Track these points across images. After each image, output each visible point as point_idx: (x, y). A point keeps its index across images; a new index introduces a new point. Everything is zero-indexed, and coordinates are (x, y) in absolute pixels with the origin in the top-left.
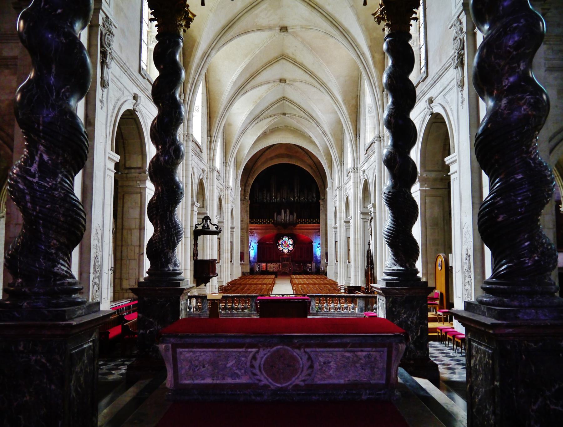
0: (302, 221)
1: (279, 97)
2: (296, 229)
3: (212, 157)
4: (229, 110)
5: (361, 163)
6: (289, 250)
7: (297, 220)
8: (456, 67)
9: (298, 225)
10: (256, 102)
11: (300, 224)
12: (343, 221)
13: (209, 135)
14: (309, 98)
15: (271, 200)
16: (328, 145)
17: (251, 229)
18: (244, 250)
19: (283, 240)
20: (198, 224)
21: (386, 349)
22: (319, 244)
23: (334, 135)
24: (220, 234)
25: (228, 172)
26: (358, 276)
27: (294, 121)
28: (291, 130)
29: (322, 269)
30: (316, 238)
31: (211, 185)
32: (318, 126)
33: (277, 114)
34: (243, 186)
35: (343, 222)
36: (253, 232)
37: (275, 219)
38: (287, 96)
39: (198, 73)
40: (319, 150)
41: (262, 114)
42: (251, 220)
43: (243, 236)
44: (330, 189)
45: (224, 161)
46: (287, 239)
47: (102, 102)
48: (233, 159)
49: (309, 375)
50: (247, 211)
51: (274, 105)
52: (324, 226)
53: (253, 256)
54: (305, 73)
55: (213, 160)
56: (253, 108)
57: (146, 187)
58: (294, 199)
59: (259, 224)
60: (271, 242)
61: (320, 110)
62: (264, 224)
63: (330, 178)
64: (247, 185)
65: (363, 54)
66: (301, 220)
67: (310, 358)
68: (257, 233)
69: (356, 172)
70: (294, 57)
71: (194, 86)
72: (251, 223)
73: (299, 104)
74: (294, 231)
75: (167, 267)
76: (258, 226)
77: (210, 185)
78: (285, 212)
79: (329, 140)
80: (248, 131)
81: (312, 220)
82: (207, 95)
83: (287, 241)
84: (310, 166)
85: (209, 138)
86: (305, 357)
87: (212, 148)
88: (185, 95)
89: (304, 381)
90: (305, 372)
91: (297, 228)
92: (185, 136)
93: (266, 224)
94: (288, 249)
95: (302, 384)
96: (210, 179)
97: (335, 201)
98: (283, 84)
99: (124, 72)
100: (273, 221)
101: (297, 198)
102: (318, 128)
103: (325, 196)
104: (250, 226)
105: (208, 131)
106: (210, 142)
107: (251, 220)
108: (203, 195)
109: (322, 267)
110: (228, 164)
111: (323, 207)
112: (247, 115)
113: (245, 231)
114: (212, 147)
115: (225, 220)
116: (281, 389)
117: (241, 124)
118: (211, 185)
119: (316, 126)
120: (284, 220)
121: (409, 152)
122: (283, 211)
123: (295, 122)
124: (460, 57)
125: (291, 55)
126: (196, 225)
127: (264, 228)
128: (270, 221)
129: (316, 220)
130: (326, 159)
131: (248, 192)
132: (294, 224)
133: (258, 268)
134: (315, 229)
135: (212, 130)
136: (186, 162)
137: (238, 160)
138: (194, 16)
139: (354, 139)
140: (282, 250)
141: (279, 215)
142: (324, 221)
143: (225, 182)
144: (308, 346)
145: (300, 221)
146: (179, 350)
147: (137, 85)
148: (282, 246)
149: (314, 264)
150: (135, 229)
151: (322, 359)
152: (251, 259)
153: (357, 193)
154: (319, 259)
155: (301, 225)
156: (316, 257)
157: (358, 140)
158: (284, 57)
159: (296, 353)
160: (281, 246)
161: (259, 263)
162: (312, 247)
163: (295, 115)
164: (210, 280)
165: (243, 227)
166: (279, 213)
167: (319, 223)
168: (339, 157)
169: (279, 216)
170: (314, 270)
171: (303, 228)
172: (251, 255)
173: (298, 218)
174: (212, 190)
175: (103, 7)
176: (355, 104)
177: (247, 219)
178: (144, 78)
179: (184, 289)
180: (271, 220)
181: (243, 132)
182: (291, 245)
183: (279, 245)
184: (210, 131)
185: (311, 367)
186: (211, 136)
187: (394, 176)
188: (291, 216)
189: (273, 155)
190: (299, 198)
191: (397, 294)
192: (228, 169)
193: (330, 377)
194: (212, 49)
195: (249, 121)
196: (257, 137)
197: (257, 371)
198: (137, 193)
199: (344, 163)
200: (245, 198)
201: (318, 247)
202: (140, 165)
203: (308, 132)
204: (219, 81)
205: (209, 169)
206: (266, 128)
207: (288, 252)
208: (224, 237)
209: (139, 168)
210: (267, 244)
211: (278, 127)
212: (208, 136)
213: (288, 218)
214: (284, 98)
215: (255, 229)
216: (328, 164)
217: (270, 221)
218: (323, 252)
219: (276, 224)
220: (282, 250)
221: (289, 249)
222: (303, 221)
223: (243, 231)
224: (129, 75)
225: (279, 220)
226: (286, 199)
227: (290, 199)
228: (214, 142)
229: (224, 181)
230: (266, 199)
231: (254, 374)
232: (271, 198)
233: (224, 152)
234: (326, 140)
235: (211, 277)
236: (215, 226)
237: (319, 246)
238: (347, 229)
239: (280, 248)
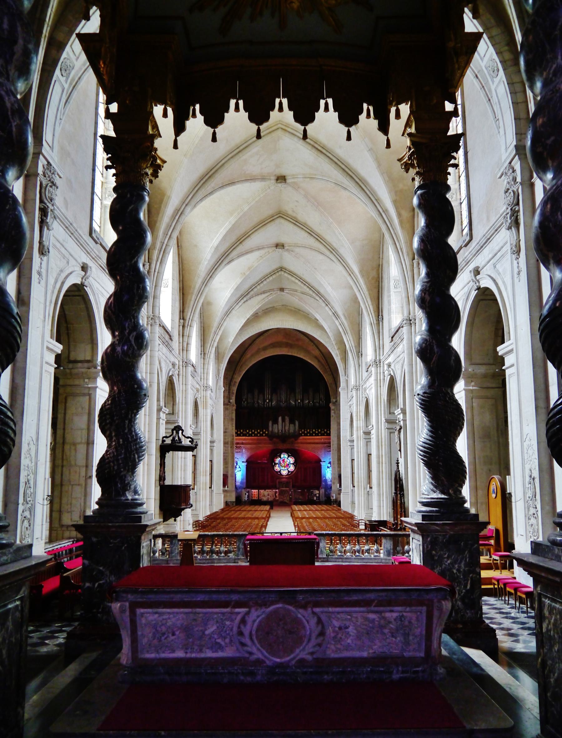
0: (306, 432)
1: (274, 267)
2: (298, 443)
3: (185, 346)
4: (209, 284)
5: (385, 354)
6: (289, 471)
7: (299, 431)
8: (509, 228)
9: (301, 438)
10: (244, 274)
11: (304, 436)
12: (362, 431)
13: (182, 318)
14: (315, 269)
15: (264, 404)
16: (341, 330)
17: (237, 443)
18: (227, 472)
19: (281, 458)
20: (166, 437)
21: (424, 608)
22: (330, 463)
23: (348, 317)
24: (195, 450)
25: (206, 366)
26: (383, 506)
27: (295, 299)
28: (291, 310)
29: (334, 498)
30: (325, 454)
31: (184, 383)
32: (327, 305)
33: (272, 290)
34: (227, 385)
35: (362, 433)
36: (240, 448)
37: (270, 429)
38: (285, 265)
39: (168, 236)
40: (328, 337)
41: (252, 290)
42: (238, 431)
43: (226, 452)
44: (344, 389)
45: (201, 352)
46: (286, 456)
47: (39, 273)
48: (214, 349)
49: (320, 645)
50: (232, 419)
51: (268, 278)
52: (336, 438)
53: (240, 480)
54: (309, 236)
55: (187, 350)
56: (240, 281)
57: (97, 387)
58: (295, 403)
59: (249, 436)
60: (265, 460)
61: (329, 284)
62: (254, 436)
63: (344, 374)
64: (232, 384)
65: (386, 211)
66: (305, 431)
67: (319, 621)
68: (245, 448)
69: (378, 366)
70: (294, 215)
71: (162, 253)
72: (238, 435)
73: (302, 276)
74: (296, 445)
75: (124, 495)
76: (248, 439)
77: (182, 384)
78: (283, 420)
79: (342, 324)
80: (233, 312)
81: (320, 431)
82: (179, 265)
83: (286, 459)
84: (316, 357)
85: (182, 321)
86: (314, 621)
87: (185, 334)
88: (150, 265)
89: (312, 653)
90: (314, 641)
91: (299, 441)
92: (150, 319)
93: (257, 436)
94: (287, 471)
95: (309, 658)
96: (183, 376)
97: (350, 405)
98: (280, 250)
99: (70, 234)
101: (299, 401)
102: (327, 308)
103: (336, 398)
104: (236, 439)
105: (180, 312)
106: (183, 326)
107: (238, 431)
108: (173, 397)
109: (334, 495)
110: (206, 355)
111: (335, 413)
112: (232, 291)
113: (229, 446)
114: (186, 333)
115: (202, 432)
116: (280, 665)
117: (225, 303)
118: (184, 383)
119: (324, 305)
120: (282, 431)
121: (450, 340)
122: (280, 419)
123: (297, 300)
124: (515, 214)
125: (290, 212)
126: (163, 437)
127: (255, 441)
129: (325, 430)
130: (338, 349)
131: (233, 393)
132: (296, 436)
133: (246, 496)
134: (325, 443)
135: (186, 310)
136: (150, 353)
137: (220, 351)
138: (164, 162)
139: (375, 322)
140: (280, 471)
141: (275, 424)
142: (336, 432)
143: (202, 380)
144: (317, 604)
145: (304, 433)
146: (140, 611)
147: (87, 251)
148: (279, 466)
149: (322, 491)
150: (81, 443)
151: (336, 624)
152: (238, 484)
153: (381, 394)
154: (329, 483)
155: (305, 437)
156: (326, 480)
157: (381, 323)
158: (281, 215)
159: (301, 614)
160: (277, 465)
161: (248, 490)
162: (320, 467)
163: (296, 291)
164: (182, 513)
165: (227, 440)
166: (276, 422)
167: (329, 435)
168: (355, 346)
169: (275, 426)
170: (323, 499)
171: (308, 441)
172: (237, 478)
173: (300, 428)
174: (185, 391)
175: (43, 151)
176: (376, 276)
177: (232, 429)
178: (96, 243)
179: (146, 526)
180: (264, 430)
181: (227, 313)
182: (291, 465)
183: (276, 464)
184: (183, 312)
185: (322, 634)
186: (185, 318)
187: (431, 371)
189: (266, 344)
190: (302, 400)
191: (437, 531)
192: (206, 362)
193: (348, 648)
194: (186, 205)
195: (234, 299)
196: (246, 319)
197: (247, 641)
198: (84, 395)
199: (362, 354)
200: (229, 402)
201: (328, 467)
202: (88, 358)
203: (314, 314)
204: (196, 246)
205: (181, 363)
206: (257, 308)
207: (288, 475)
208: (201, 454)
209: (88, 361)
211: (274, 307)
212: (180, 319)
213: (287, 428)
214: (282, 269)
215: (243, 444)
216: (340, 356)
218: (335, 474)
219: (272, 436)
220: (280, 471)
221: (289, 469)
222: (308, 433)
223: (227, 445)
224: (76, 239)
225: (276, 431)
226: (285, 402)
227: (290, 402)
228: (189, 327)
229: (201, 379)
230: (258, 402)
231: (243, 645)
232: (264, 401)
233: (201, 340)
234: (338, 324)
235: (184, 509)
236: (189, 439)
237: (329, 465)
238: (367, 442)
239: (277, 468)
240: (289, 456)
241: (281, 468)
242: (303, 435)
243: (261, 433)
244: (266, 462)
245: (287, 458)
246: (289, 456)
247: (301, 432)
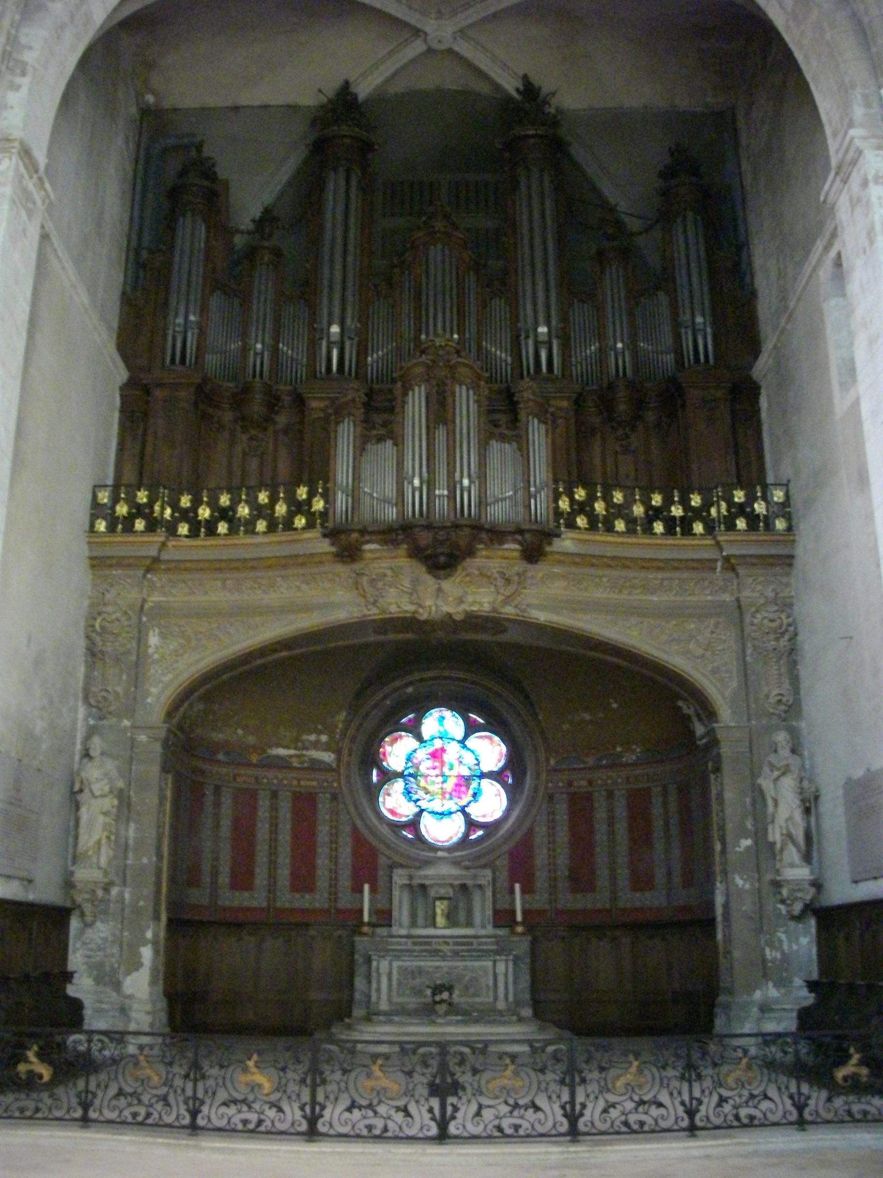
0: (599, 507)
6: (471, 824)
7: (557, 497)
19: (419, 738)
37: (343, 472)
60: (316, 745)
100: (319, 505)
128: (298, 507)
140: (414, 824)
141: (380, 439)
148: (408, 792)
160: (398, 786)
183: (388, 776)
188: (495, 446)
207: (464, 841)
210: (283, 764)
217: (298, 507)
220: (414, 824)
240: (471, 728)
241: (423, 804)
242: (581, 521)
243: (281, 509)
244: (327, 757)
245: (462, 742)
246: (471, 728)
247: (564, 504)
